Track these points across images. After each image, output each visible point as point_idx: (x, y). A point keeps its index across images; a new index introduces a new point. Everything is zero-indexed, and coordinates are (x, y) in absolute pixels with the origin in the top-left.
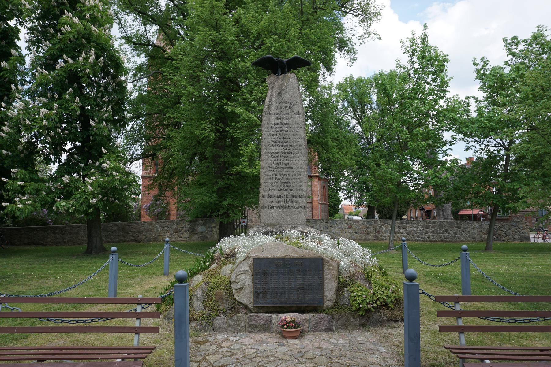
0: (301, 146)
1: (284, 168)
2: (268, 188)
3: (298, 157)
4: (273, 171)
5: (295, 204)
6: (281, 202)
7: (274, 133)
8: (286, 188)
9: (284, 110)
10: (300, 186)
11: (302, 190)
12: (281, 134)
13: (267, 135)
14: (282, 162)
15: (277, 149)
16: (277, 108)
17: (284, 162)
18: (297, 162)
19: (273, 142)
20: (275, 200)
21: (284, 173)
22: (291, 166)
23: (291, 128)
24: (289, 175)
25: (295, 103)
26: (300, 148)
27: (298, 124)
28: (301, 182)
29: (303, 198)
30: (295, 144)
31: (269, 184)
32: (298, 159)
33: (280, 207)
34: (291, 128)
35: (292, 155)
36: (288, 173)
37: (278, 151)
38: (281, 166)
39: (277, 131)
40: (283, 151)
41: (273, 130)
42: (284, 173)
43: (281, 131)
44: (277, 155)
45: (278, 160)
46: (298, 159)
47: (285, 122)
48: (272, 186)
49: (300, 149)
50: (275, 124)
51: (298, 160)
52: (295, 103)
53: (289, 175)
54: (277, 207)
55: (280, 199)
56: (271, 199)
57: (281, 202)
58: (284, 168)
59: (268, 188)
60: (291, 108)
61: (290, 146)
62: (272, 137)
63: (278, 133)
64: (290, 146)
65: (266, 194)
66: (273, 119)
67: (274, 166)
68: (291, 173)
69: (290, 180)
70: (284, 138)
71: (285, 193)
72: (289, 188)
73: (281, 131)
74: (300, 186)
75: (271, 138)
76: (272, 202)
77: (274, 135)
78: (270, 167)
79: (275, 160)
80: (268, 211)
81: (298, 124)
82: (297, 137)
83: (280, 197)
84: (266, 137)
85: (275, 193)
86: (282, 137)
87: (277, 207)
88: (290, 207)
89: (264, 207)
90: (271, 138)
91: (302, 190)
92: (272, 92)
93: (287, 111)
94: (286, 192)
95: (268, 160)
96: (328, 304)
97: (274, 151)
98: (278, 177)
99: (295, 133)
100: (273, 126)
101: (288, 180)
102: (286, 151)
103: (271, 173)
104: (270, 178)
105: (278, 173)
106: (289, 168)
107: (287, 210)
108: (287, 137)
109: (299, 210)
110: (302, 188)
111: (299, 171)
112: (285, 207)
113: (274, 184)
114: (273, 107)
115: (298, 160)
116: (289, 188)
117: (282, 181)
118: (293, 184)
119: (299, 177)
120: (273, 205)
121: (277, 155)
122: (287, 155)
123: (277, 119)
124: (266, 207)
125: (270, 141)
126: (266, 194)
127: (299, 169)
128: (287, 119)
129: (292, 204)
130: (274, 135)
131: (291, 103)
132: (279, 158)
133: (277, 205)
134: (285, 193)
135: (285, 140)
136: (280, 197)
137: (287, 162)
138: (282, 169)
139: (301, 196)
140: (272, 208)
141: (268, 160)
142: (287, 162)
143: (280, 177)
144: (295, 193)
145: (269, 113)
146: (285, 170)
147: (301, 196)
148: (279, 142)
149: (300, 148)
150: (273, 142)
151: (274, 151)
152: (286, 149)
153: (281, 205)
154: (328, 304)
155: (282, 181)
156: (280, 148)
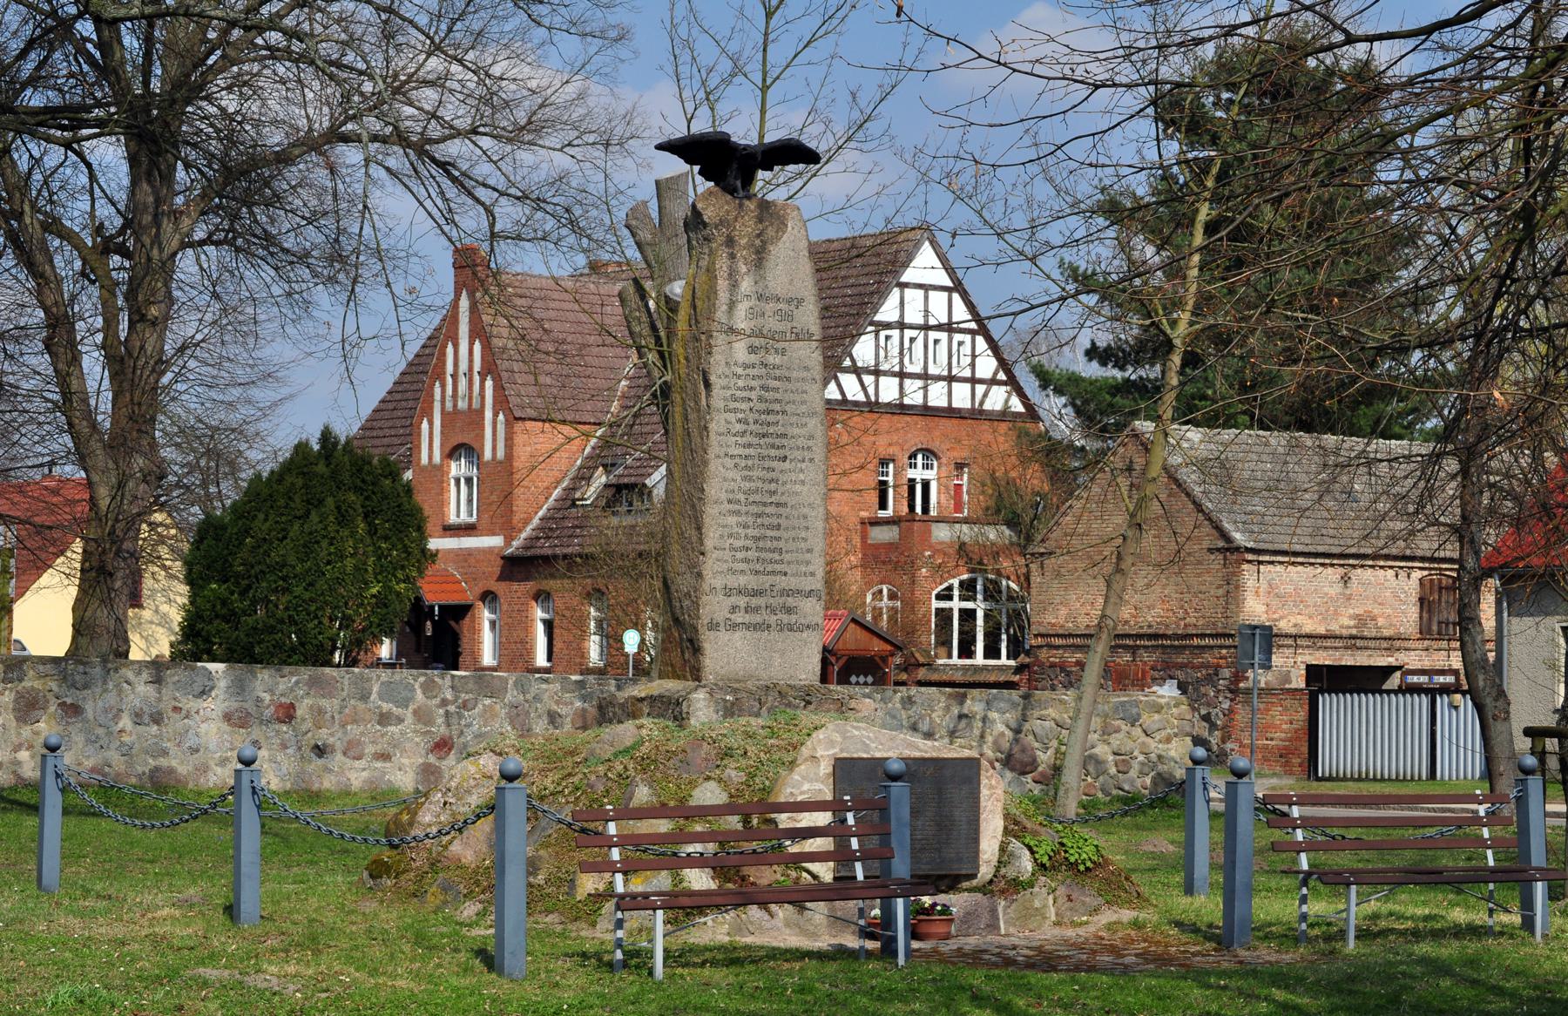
0: (811, 437)
1: (765, 504)
2: (725, 566)
3: (802, 471)
4: (738, 513)
5: (793, 618)
6: (757, 609)
7: (745, 394)
8: (769, 568)
9: (773, 324)
10: (808, 563)
11: (812, 574)
12: (760, 399)
13: (725, 399)
14: (760, 484)
15: (750, 445)
16: (753, 314)
17: (766, 487)
18: (798, 488)
19: (739, 421)
20: (742, 601)
21: (767, 521)
22: (783, 499)
23: (788, 379)
24: (778, 527)
25: (800, 301)
26: (810, 443)
27: (806, 368)
28: (809, 551)
29: (813, 600)
30: (796, 431)
31: (727, 555)
32: (802, 476)
33: (756, 627)
34: (788, 379)
35: (787, 465)
36: (775, 521)
37: (751, 451)
38: (757, 498)
39: (752, 389)
40: (765, 452)
41: (741, 383)
42: (767, 521)
43: (762, 387)
44: (750, 463)
45: (750, 479)
46: (802, 476)
47: (773, 359)
48: (735, 560)
49: (809, 448)
50: (746, 366)
51: (803, 482)
52: (800, 301)
53: (778, 527)
54: (748, 626)
55: (755, 601)
56: (733, 599)
57: (757, 609)
58: (765, 504)
59: (725, 566)
60: (789, 317)
61: (784, 436)
62: (737, 405)
63: (753, 395)
64: (784, 436)
65: (718, 583)
66: (740, 350)
67: (742, 497)
68: (782, 521)
69: (781, 544)
70: (769, 412)
71: (767, 581)
72: (778, 567)
73: (762, 387)
74: (808, 563)
75: (735, 411)
76: (734, 609)
77: (743, 399)
78: (730, 502)
79: (745, 478)
80: (723, 636)
81: (806, 368)
82: (803, 408)
83: (757, 593)
84: (721, 404)
85: (742, 580)
86: (763, 406)
87: (748, 626)
88: (781, 627)
89: (713, 626)
90: (735, 411)
91: (812, 574)
92: (732, 256)
93: (780, 327)
94: (770, 579)
95: (725, 480)
96: (985, 871)
97: (741, 451)
98: (750, 532)
99: (797, 398)
100: (740, 371)
101: (775, 543)
102: (773, 452)
103: (732, 520)
104: (730, 536)
105: (750, 520)
106: (778, 505)
107: (774, 635)
108: (777, 407)
109: (805, 635)
110: (811, 568)
111: (805, 517)
112: (769, 626)
113: (739, 555)
114: (742, 308)
115: (803, 482)
116: (778, 567)
117: (761, 544)
118: (787, 557)
119: (803, 534)
120: (739, 618)
121: (750, 463)
122: (775, 464)
123: (752, 350)
124: (718, 624)
125: (732, 417)
126: (718, 583)
127: (806, 511)
128: (776, 351)
129: (785, 618)
130: (743, 399)
131: (789, 301)
132: (755, 474)
133: (747, 618)
134: (767, 581)
135: (771, 418)
136: (757, 593)
137: (773, 486)
138: (761, 508)
139: (810, 593)
140: (734, 627)
141: (725, 480)
142: (773, 486)
143: (756, 533)
144: (792, 582)
145: (732, 330)
146: (768, 510)
147: (810, 593)
148: (756, 422)
149: (810, 443)
150: (739, 421)
151: (741, 451)
152: (773, 446)
153: (757, 619)
154: (985, 871)
155: (761, 544)
156: (755, 441)
